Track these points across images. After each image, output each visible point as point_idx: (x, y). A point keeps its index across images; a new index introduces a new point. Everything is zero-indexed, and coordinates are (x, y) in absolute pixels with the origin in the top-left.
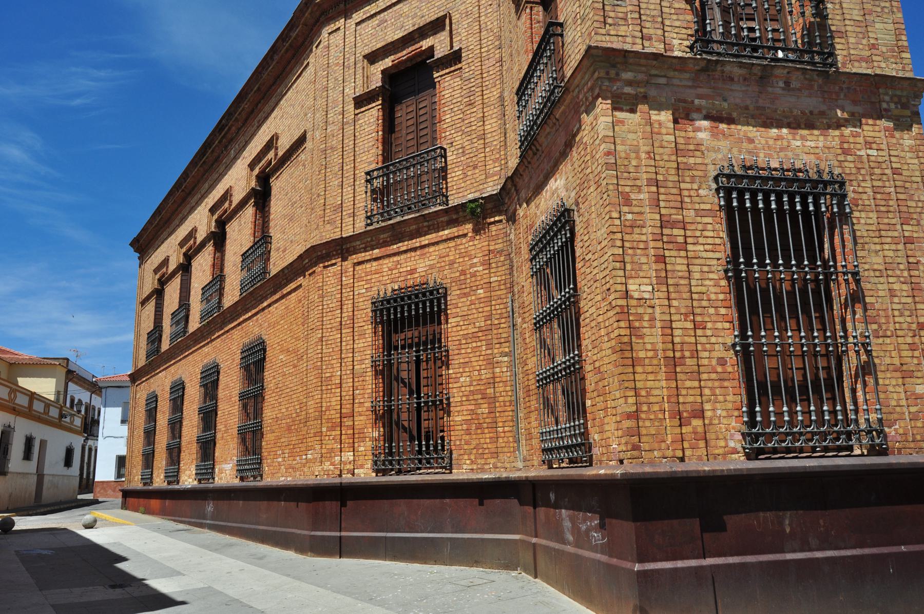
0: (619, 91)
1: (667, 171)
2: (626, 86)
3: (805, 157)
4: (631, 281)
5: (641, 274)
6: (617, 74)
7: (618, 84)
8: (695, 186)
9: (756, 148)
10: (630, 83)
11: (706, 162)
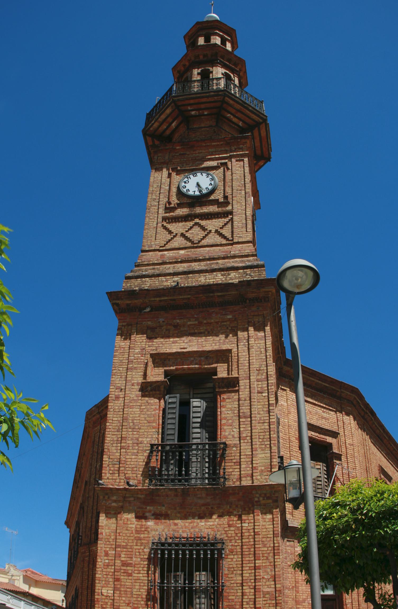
0: (110, 505)
1: (128, 541)
2: (113, 502)
3: (206, 530)
4: (104, 588)
5: (109, 586)
6: (109, 498)
7: (110, 502)
8: (142, 547)
9: (178, 528)
10: (115, 501)
11: (150, 536)
